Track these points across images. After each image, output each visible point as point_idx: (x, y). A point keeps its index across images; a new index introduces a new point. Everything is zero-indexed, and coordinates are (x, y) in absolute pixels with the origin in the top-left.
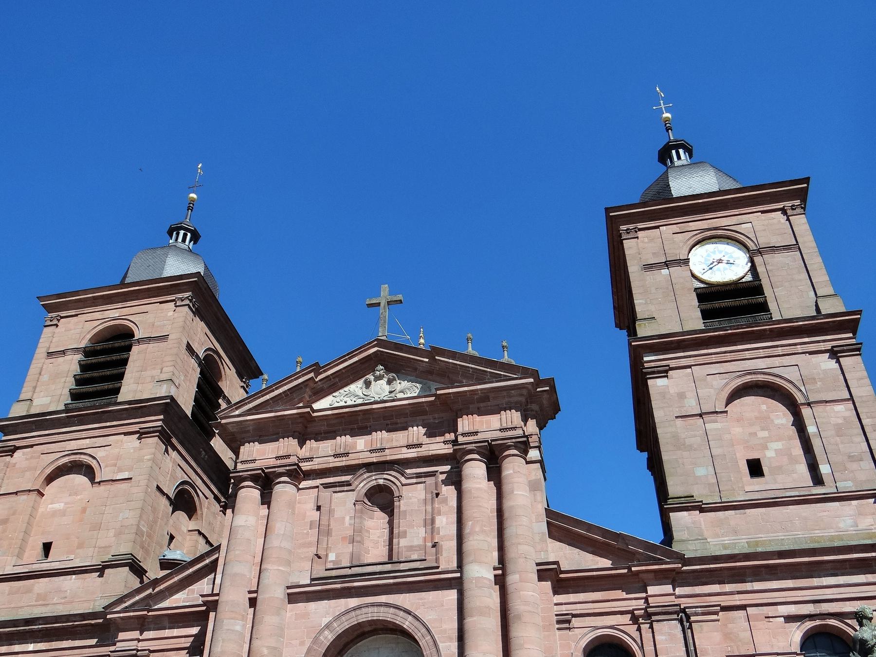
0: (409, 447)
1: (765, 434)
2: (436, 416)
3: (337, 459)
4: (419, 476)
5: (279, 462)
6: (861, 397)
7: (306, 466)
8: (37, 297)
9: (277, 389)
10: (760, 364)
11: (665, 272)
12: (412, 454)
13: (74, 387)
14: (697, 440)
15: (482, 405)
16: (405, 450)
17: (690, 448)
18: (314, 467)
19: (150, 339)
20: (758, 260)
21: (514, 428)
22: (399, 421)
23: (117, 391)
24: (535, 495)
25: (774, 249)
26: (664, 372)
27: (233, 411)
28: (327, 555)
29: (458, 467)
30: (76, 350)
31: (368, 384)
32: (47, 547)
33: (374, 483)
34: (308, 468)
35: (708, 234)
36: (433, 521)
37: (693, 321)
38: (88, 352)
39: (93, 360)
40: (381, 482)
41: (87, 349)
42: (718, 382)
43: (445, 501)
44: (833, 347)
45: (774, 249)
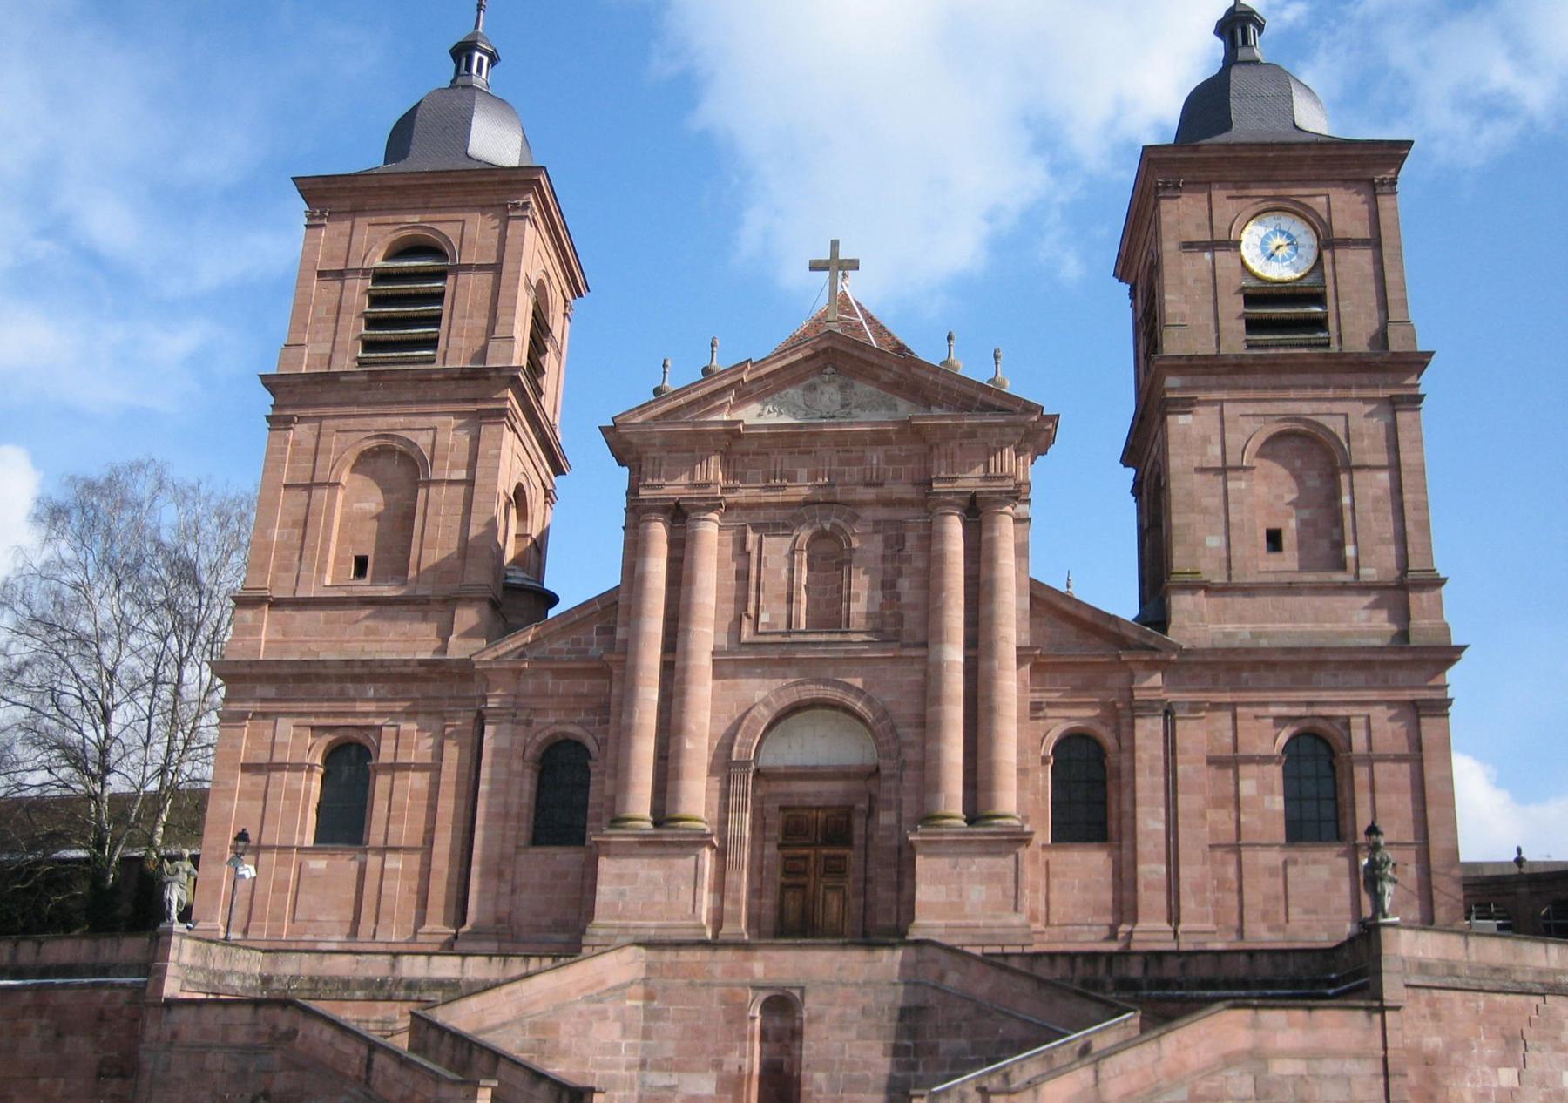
0: (868, 484)
2: (904, 447)
4: (877, 523)
5: (695, 493)
6: (1410, 465)
8: (293, 179)
9: (695, 390)
10: (1305, 408)
11: (1207, 256)
13: (364, 331)
14: (1215, 502)
15: (965, 441)
16: (860, 489)
17: (1205, 511)
18: (740, 500)
19: (468, 268)
20: (1327, 255)
21: (1003, 478)
22: (853, 448)
23: (432, 343)
24: (1020, 562)
25: (1347, 242)
26: (1186, 406)
27: (634, 416)
29: (928, 517)
34: (733, 500)
35: (1271, 204)
36: (893, 585)
37: (1235, 340)
38: (381, 276)
39: (384, 288)
42: (1249, 426)
43: (909, 559)
44: (1392, 396)
45: (1347, 242)
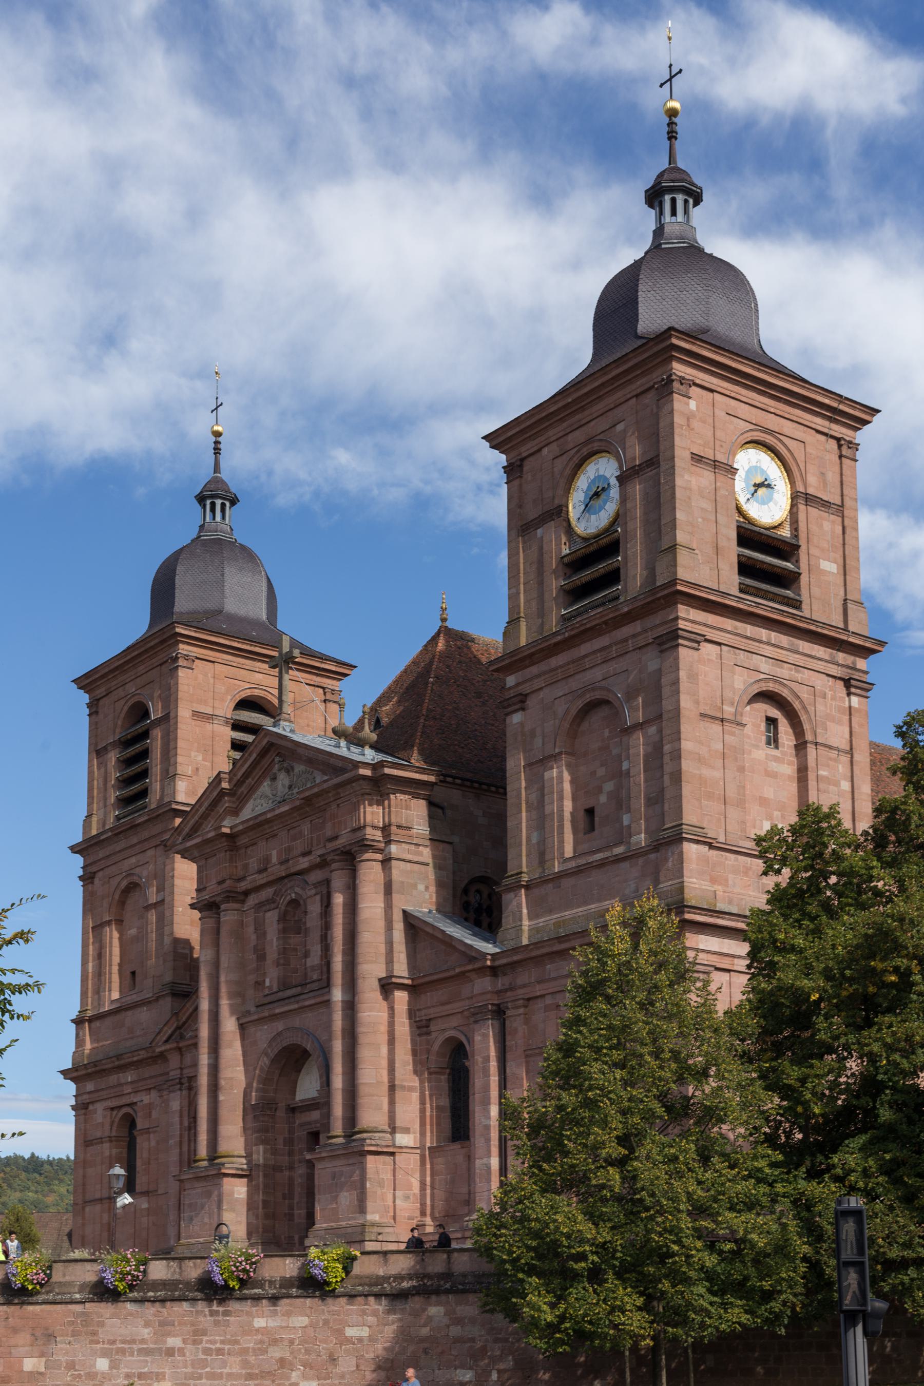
0: (305, 854)
1: (601, 772)
3: (261, 876)
7: (243, 886)
12: (304, 863)
15: (339, 802)
16: (301, 859)
28: (264, 981)
30: (114, 744)
31: (274, 779)
32: (133, 973)
33: (288, 898)
40: (293, 896)
41: (122, 739)
